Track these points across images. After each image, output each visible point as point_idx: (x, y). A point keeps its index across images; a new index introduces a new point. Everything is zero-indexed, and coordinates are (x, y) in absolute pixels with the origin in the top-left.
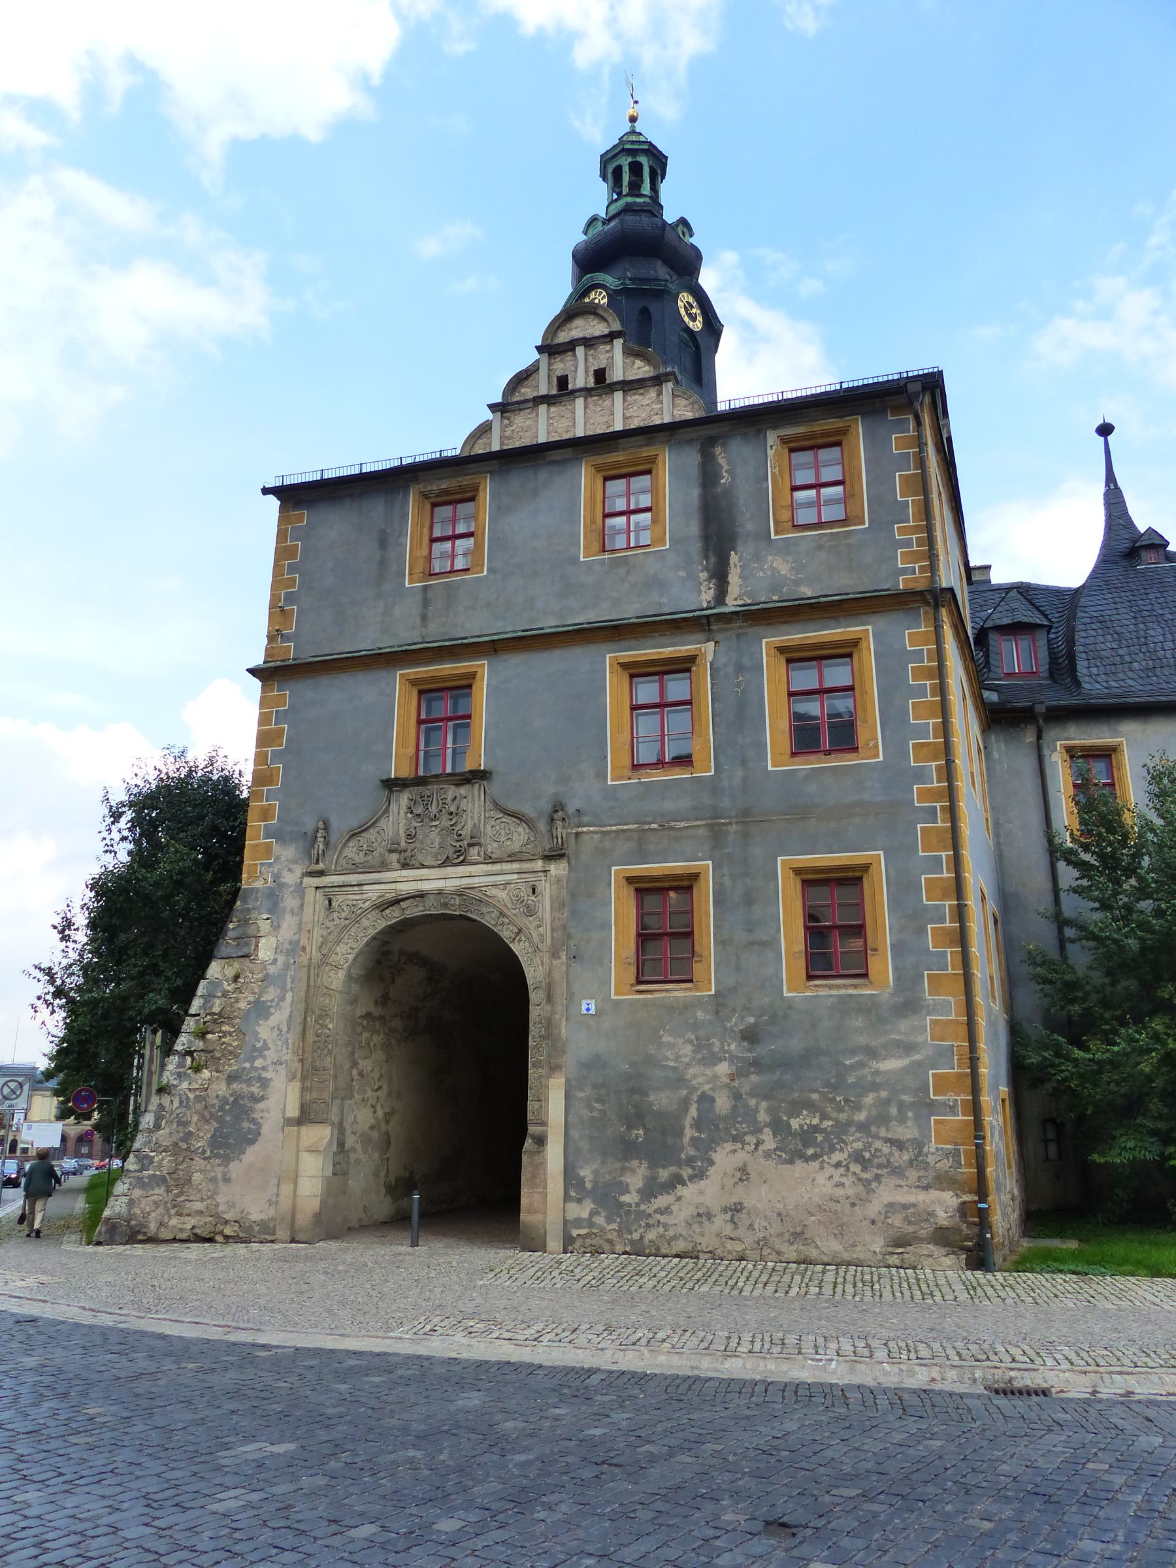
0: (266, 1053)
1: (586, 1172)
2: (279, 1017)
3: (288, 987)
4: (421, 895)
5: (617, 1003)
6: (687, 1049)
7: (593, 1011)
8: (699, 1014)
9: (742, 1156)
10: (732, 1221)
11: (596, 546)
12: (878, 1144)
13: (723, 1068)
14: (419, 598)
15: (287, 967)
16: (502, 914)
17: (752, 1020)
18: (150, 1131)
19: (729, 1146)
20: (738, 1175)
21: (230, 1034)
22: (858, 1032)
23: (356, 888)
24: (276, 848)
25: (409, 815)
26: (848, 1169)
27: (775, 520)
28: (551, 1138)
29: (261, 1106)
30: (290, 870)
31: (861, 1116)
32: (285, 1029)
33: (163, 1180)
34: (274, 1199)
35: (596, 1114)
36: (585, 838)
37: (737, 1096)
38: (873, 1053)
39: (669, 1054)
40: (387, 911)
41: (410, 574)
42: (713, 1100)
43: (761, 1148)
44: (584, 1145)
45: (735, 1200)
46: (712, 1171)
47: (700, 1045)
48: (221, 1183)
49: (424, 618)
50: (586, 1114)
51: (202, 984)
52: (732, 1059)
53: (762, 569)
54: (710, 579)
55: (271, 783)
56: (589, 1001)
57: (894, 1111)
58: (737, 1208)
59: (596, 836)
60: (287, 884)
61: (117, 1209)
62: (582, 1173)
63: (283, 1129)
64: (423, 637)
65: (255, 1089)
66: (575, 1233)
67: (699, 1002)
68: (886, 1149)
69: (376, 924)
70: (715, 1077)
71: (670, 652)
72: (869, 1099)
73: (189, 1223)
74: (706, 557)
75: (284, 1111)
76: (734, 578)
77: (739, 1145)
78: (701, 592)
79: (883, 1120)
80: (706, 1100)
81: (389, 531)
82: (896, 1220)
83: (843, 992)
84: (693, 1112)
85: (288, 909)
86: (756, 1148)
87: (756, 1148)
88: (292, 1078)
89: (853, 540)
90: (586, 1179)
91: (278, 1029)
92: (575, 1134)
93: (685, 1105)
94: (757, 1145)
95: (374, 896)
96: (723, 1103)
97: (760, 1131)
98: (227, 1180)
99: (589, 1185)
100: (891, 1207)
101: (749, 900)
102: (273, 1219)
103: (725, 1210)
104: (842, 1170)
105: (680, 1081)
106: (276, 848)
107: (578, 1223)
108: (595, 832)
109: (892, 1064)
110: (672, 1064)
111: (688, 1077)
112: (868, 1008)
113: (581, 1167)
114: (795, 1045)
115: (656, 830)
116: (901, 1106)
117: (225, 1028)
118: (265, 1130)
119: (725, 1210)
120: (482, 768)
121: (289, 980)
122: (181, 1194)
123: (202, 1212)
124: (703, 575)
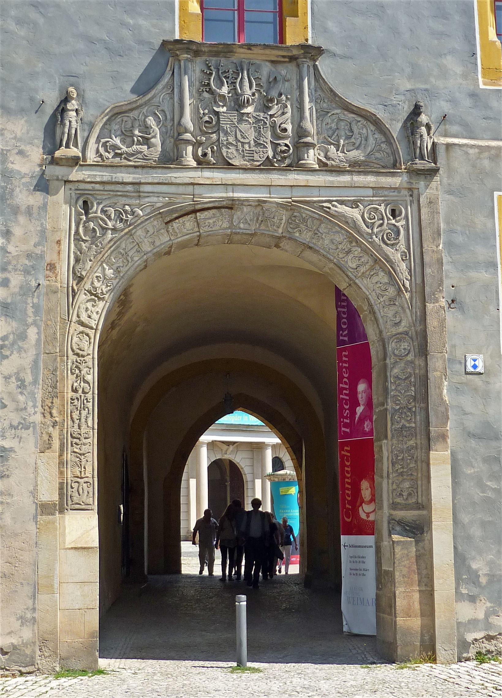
3: (30, 320)
16: (352, 239)
23: (129, 188)
25: (206, 95)
28: (435, 524)
30: (21, 153)
32: (29, 378)
34: (29, 615)
35: (490, 494)
36: (458, 152)
40: (175, 224)
44: (476, 532)
50: (477, 494)
56: (474, 357)
59: (471, 151)
60: (19, 172)
62: (474, 566)
63: (35, 517)
66: (470, 637)
75: (34, 493)
85: (23, 208)
90: (480, 573)
91: (18, 379)
92: (465, 518)
95: (159, 201)
99: (483, 580)
102: (25, 645)
107: (473, 623)
108: (472, 146)
113: (474, 559)
120: (310, 42)
121: (30, 311)
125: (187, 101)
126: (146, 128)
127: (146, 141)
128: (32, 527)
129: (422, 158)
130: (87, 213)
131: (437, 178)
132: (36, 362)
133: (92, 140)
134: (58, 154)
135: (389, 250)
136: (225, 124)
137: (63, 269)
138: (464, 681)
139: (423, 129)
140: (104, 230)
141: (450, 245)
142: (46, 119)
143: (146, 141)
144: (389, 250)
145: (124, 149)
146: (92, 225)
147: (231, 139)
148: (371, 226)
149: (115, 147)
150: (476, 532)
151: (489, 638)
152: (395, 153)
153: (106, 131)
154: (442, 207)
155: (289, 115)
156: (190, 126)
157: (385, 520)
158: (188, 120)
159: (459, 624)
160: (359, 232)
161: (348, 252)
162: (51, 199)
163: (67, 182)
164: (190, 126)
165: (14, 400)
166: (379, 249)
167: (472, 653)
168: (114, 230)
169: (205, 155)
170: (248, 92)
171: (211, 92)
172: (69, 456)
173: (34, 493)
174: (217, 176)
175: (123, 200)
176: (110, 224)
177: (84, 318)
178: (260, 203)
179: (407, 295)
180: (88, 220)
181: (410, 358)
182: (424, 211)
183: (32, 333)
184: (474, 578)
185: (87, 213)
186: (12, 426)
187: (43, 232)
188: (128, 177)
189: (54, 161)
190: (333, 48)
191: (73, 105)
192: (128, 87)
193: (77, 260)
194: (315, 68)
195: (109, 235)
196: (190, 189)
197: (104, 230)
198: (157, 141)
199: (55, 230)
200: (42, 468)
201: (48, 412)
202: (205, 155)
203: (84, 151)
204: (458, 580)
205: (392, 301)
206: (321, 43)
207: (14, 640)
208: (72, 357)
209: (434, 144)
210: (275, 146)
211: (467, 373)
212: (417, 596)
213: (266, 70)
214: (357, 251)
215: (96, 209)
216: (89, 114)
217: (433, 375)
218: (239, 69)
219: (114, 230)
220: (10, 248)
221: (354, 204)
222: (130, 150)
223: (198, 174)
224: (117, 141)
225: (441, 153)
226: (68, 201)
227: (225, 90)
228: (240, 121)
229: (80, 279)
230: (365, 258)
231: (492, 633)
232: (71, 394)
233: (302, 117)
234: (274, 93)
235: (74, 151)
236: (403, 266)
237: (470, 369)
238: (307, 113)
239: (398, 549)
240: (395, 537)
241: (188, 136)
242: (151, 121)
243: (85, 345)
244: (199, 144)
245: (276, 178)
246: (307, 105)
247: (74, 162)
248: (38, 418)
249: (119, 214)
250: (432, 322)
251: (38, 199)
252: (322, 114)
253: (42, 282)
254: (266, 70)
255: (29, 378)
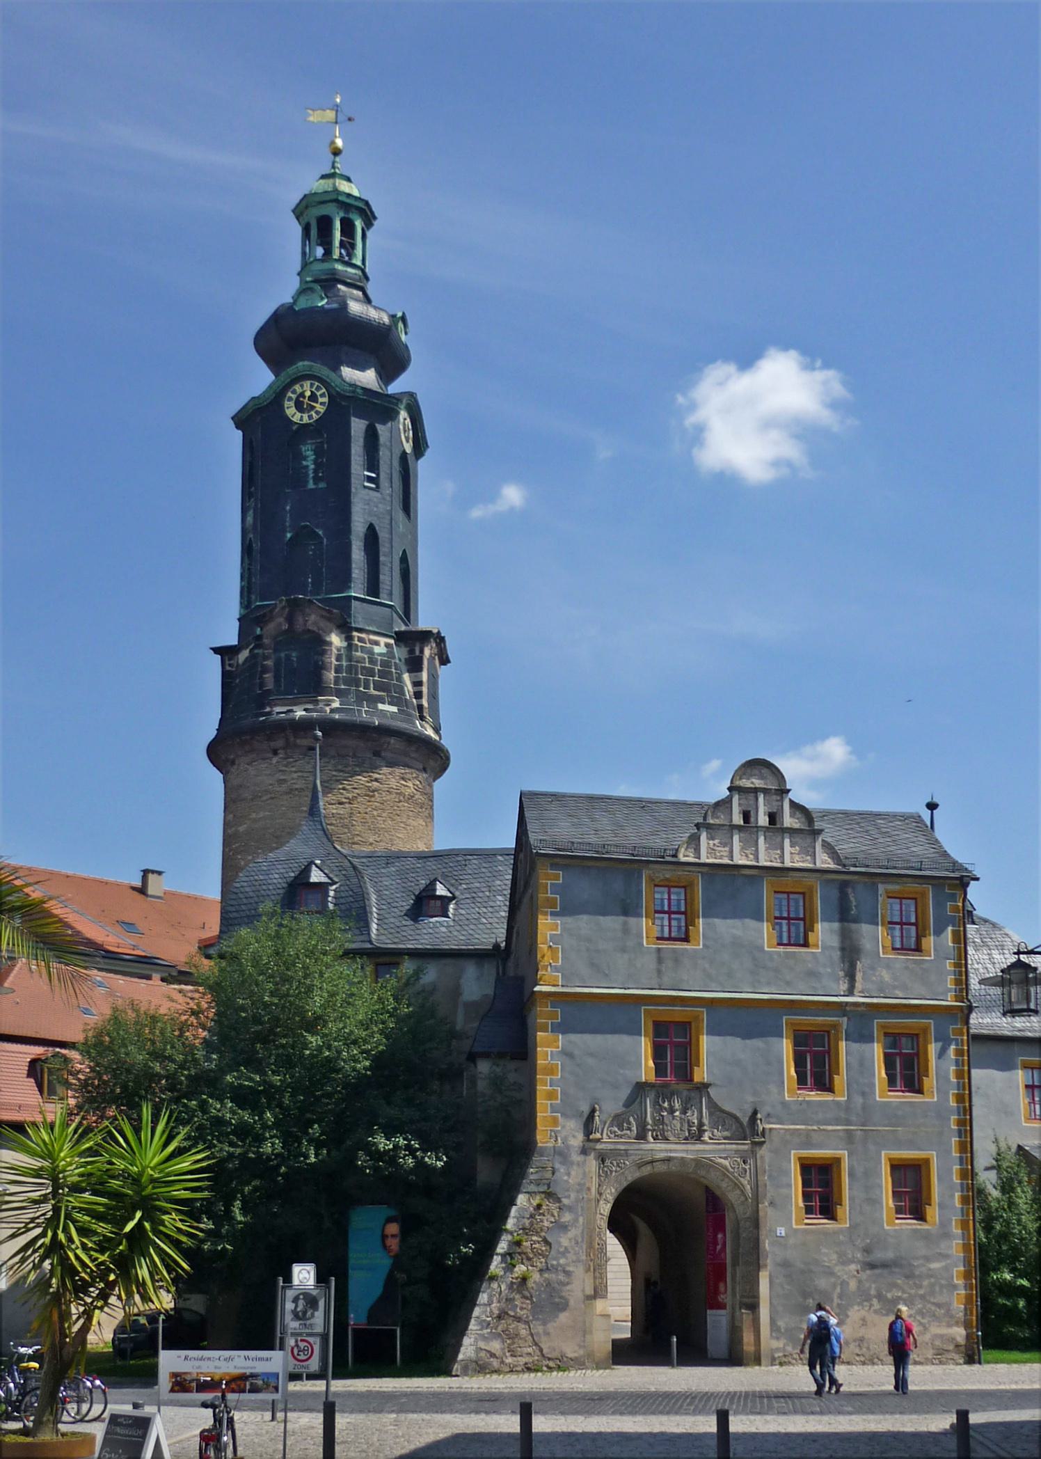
0: (568, 1255)
1: (781, 1323)
2: (573, 1233)
4: (669, 1160)
5: (796, 1230)
6: (835, 1257)
7: (783, 1234)
8: (841, 1237)
9: (863, 1313)
10: (859, 1346)
11: (775, 941)
12: (929, 1306)
13: (853, 1267)
14: (654, 956)
15: (577, 1201)
17: (868, 1241)
18: (485, 1305)
19: (856, 1308)
20: (861, 1322)
21: (539, 1242)
22: (921, 1249)
24: (561, 1120)
26: (915, 1317)
27: (883, 946)
29: (568, 1287)
30: (574, 1136)
31: (921, 1292)
32: (580, 1240)
33: (499, 1335)
36: (774, 1133)
37: (860, 1282)
38: (928, 1259)
39: (825, 1259)
41: (647, 937)
42: (848, 1283)
43: (872, 1309)
44: (780, 1309)
45: (861, 1335)
46: (848, 1321)
47: (841, 1255)
48: (542, 1337)
49: (659, 972)
51: (514, 1209)
52: (859, 1262)
53: (875, 976)
54: (846, 976)
55: (552, 1074)
57: (937, 1289)
58: (862, 1340)
61: (468, 1354)
63: (584, 1302)
64: (660, 985)
65: (562, 1277)
66: (776, 1355)
67: (841, 1231)
68: (933, 1308)
69: (632, 1175)
70: (850, 1271)
71: (822, 1021)
72: (925, 1283)
73: (522, 1360)
74: (843, 962)
75: (583, 1291)
76: (859, 976)
77: (860, 1307)
78: (839, 984)
79: (932, 1293)
80: (844, 1284)
81: (628, 901)
82: (938, 1343)
83: (914, 1227)
84: (838, 1290)
86: (870, 1309)
87: (870, 1309)
88: (588, 1270)
89: (925, 966)
93: (834, 1286)
94: (870, 1307)
96: (853, 1285)
97: (871, 1299)
98: (547, 1334)
99: (783, 1330)
100: (936, 1336)
101: (866, 1174)
103: (855, 1341)
104: (912, 1319)
105: (830, 1273)
106: (561, 1120)
107: (778, 1350)
109: (935, 1265)
110: (826, 1264)
111: (836, 1271)
112: (926, 1236)
114: (890, 1255)
115: (814, 1130)
116: (942, 1286)
117: (534, 1238)
118: (572, 1303)
119: (855, 1341)
121: (580, 1209)
122: (514, 1343)
123: (530, 1354)
124: (842, 974)
125: (649, 1110)
126: (629, 1123)
127: (629, 1129)
128: (583, 1306)
129: (758, 1135)
130: (603, 1163)
131: (765, 1146)
132: (583, 1232)
133: (605, 1129)
134: (591, 1137)
135: (742, 1179)
136: (666, 1121)
137: (593, 1190)
138: (776, 1371)
139: (759, 1121)
140: (611, 1172)
141: (770, 1177)
142: (584, 1119)
143: (629, 1129)
144: (742, 1179)
145: (619, 1133)
146: (606, 1169)
147: (669, 1128)
148: (733, 1168)
149: (615, 1132)
150: (780, 1309)
151: (785, 1356)
152: (744, 1131)
153: (611, 1125)
154: (767, 1160)
155: (695, 1115)
156: (650, 1122)
157: (738, 1302)
158: (649, 1120)
159: (772, 1349)
160: (727, 1170)
161: (722, 1180)
162: (588, 1158)
163: (595, 1149)
164: (650, 1122)
165: (573, 1249)
166: (737, 1179)
167: (777, 1362)
168: (616, 1172)
169: (657, 1136)
170: (677, 1105)
171: (660, 1105)
172: (597, 1275)
173: (583, 1291)
174: (663, 1146)
175: (620, 1158)
176: (614, 1169)
177: (602, 1211)
178: (682, 1158)
179: (750, 1200)
180: (604, 1167)
181: (751, 1229)
182: (758, 1161)
183: (581, 1219)
184: (778, 1330)
185: (603, 1163)
186: (573, 1262)
187: (584, 1173)
188: (622, 1147)
189: (589, 1140)
190: (716, 1082)
191: (597, 1113)
192: (621, 1104)
193: (599, 1185)
194: (708, 1092)
195: (614, 1174)
196: (650, 1152)
197: (611, 1172)
198: (634, 1128)
199: (590, 1172)
200: (586, 1281)
201: (588, 1255)
202: (657, 1136)
203: (602, 1135)
204: (772, 1330)
205: (743, 1203)
206: (711, 1080)
207: (576, 1355)
208: (598, 1230)
209: (763, 1128)
210: (689, 1131)
211: (777, 1236)
212: (753, 1337)
213: (685, 1093)
214: (727, 1180)
215: (608, 1162)
216: (604, 1117)
217: (762, 1238)
218: (672, 1094)
219: (616, 1172)
220: (570, 1181)
221: (725, 1158)
222: (622, 1133)
223: (654, 1145)
224: (616, 1129)
225: (767, 1132)
226: (595, 1159)
227: (666, 1105)
228: (673, 1119)
229: (601, 1194)
230: (730, 1183)
231: (786, 1354)
232: (597, 1246)
233: (702, 1116)
234: (689, 1106)
235: (598, 1135)
236: (749, 1187)
237: (778, 1234)
238: (704, 1114)
239: (744, 1316)
240: (743, 1311)
241: (649, 1127)
242: (631, 1119)
243: (602, 1224)
244: (654, 1130)
245: (690, 1147)
246: (704, 1110)
247: (598, 1140)
248: (584, 1258)
249: (618, 1165)
250: (761, 1214)
251: (580, 1158)
252: (711, 1114)
253: (585, 1196)
254: (685, 1093)
255: (580, 1240)
